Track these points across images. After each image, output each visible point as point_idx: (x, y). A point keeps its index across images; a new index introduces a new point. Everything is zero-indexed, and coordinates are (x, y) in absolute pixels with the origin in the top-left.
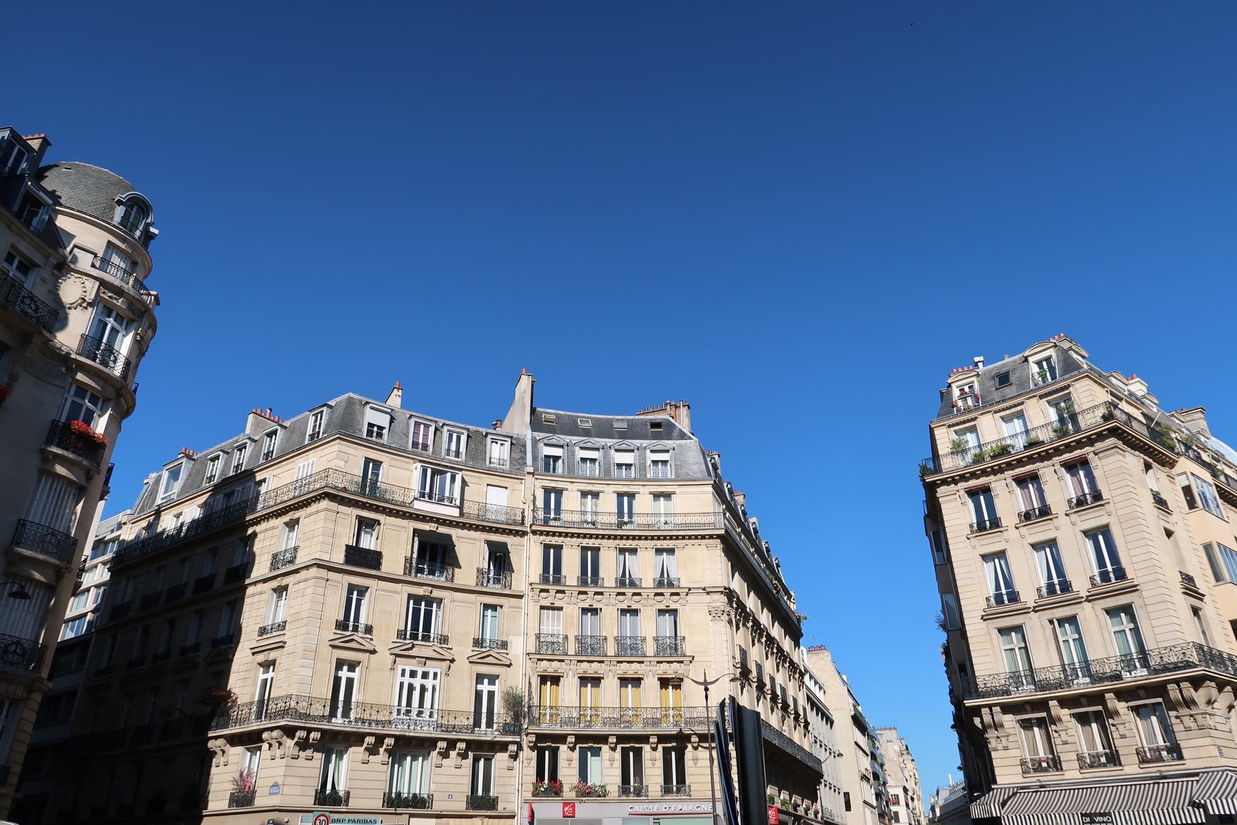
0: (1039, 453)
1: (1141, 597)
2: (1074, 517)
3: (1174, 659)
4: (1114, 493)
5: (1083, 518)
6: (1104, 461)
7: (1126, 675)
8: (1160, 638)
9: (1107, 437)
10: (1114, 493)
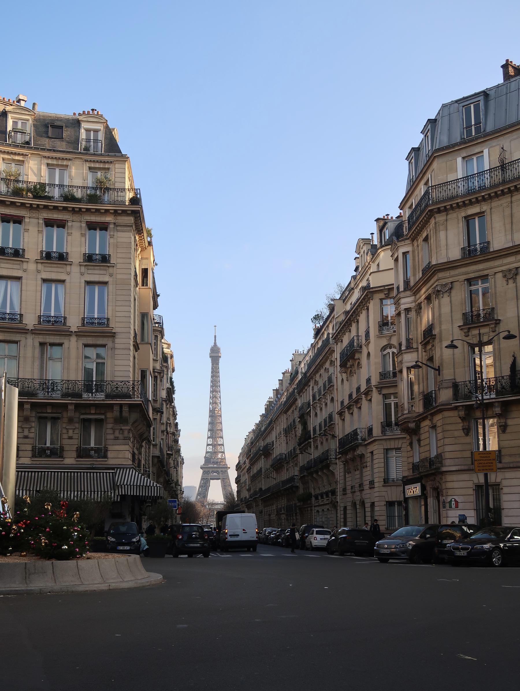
0: (73, 208)
1: (113, 342)
2: (83, 268)
3: (125, 390)
4: (119, 260)
6: (120, 234)
7: (85, 396)
8: (117, 374)
10: (119, 260)
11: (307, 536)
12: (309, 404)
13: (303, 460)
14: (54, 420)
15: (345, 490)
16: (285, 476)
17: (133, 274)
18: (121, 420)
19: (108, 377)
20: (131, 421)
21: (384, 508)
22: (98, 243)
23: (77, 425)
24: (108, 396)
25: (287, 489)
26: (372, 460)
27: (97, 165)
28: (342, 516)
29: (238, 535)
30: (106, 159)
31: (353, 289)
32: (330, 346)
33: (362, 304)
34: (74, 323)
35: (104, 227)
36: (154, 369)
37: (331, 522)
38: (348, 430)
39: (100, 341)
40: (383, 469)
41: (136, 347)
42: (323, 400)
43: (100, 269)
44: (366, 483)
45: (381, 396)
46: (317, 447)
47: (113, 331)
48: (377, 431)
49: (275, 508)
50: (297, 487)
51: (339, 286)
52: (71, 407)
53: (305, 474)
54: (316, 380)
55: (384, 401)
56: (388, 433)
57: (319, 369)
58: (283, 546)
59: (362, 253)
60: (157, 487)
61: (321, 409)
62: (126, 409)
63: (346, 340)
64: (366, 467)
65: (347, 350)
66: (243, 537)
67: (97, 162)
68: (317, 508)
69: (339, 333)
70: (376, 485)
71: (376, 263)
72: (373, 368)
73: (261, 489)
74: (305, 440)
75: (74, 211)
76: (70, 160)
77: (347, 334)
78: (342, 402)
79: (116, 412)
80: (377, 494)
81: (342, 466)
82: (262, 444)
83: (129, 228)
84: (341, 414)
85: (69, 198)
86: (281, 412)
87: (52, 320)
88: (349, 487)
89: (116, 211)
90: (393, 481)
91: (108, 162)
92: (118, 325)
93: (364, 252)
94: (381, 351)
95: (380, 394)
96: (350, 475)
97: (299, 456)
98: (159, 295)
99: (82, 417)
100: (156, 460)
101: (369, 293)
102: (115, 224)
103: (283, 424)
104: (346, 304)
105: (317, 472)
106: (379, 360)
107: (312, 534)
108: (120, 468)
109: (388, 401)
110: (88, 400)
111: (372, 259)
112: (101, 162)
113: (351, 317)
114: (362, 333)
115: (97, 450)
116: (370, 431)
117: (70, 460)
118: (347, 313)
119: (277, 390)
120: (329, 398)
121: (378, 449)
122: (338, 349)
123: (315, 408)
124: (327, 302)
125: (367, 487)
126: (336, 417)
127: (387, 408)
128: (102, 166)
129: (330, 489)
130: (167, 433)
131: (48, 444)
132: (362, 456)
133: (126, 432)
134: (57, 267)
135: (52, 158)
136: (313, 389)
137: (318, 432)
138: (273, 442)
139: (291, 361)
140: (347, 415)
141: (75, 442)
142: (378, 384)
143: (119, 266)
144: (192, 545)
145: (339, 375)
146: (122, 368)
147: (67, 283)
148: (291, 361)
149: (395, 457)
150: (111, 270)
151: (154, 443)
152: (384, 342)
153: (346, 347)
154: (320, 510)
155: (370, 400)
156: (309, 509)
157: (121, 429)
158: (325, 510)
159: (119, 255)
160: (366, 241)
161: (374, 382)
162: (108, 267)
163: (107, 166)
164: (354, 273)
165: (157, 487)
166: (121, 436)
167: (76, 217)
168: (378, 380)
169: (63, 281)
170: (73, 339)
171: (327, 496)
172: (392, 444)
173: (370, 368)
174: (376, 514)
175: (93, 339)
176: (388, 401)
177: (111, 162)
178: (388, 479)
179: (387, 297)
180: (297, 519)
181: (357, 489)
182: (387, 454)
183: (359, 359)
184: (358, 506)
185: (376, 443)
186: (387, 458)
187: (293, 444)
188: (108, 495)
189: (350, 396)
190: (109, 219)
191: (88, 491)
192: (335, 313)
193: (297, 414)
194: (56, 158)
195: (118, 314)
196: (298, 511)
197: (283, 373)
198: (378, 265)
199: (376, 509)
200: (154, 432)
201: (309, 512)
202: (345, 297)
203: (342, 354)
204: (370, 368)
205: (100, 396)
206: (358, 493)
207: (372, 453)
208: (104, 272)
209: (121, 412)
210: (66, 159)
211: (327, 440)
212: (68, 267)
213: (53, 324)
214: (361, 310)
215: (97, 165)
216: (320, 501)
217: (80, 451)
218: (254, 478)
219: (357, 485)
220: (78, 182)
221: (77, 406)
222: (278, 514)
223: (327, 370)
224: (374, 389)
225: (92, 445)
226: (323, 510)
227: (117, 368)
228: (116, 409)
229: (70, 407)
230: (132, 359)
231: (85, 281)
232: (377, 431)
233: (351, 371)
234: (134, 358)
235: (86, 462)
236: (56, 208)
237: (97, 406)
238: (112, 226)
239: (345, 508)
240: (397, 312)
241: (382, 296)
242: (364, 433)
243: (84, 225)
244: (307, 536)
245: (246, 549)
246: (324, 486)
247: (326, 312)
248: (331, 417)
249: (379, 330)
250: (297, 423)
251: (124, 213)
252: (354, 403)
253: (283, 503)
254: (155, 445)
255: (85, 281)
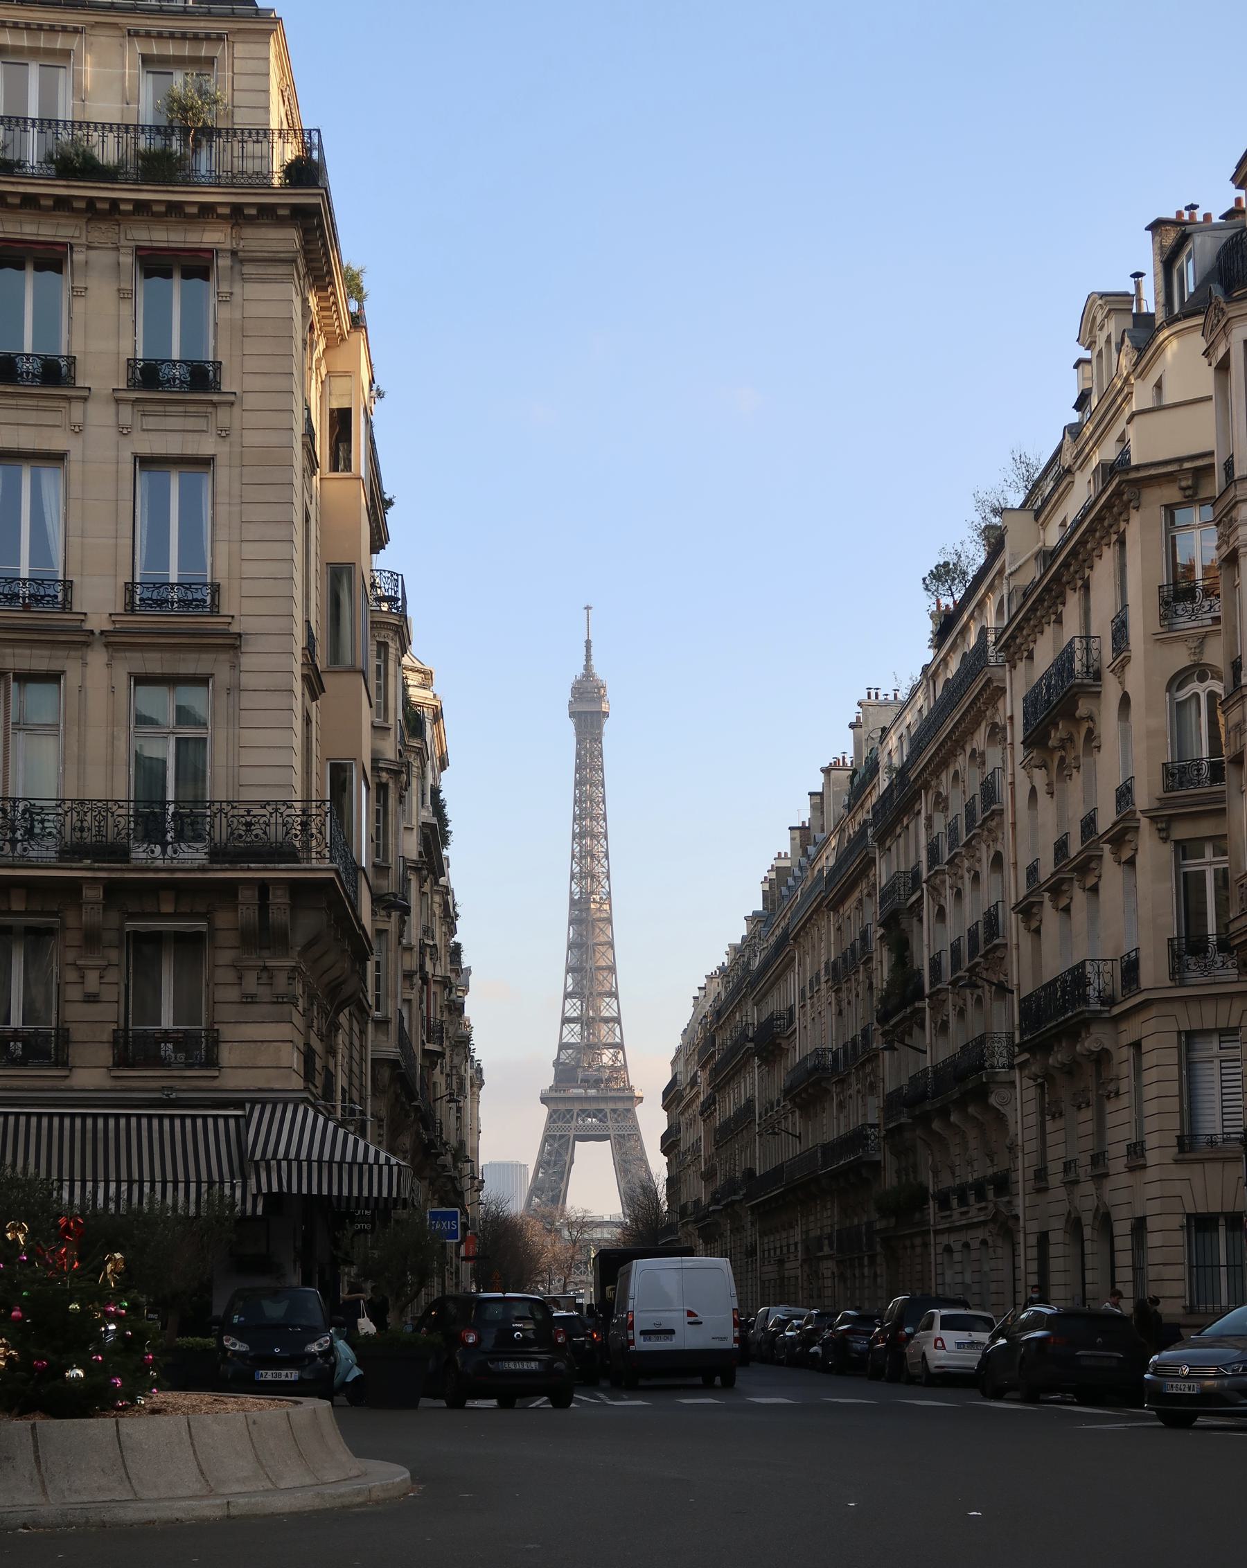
0: (91, 201)
1: (235, 666)
2: (126, 412)
4: (252, 383)
5: (151, 422)
6: (253, 290)
7: (139, 853)
8: (248, 776)
9: (280, 222)
10: (252, 383)
11: (910, 1336)
12: (916, 875)
13: (894, 1071)
14: (37, 937)
15: (1041, 1174)
16: (831, 1125)
17: (299, 429)
18: (264, 937)
19: (217, 788)
20: (299, 939)
21: (1180, 1238)
22: (178, 322)
23: (114, 955)
24: (217, 855)
25: (840, 1174)
26: (1138, 1071)
27: (171, 49)
28: (1033, 1266)
29: (672, 1332)
30: (201, 26)
31: (1069, 471)
32: (989, 673)
33: (1103, 524)
34: (98, 602)
35: (197, 266)
36: (375, 761)
37: (993, 1287)
38: (1054, 967)
39: (190, 665)
40: (1174, 1104)
41: (314, 686)
42: (966, 864)
43: (186, 415)
44: (1117, 1153)
45: (1169, 847)
46: (943, 1028)
47: (235, 629)
48: (1153, 972)
49: (798, 1238)
50: (876, 1167)
51: (1021, 460)
52: (92, 894)
53: (903, 1120)
54: (939, 794)
55: (1178, 866)
56: (1194, 977)
57: (952, 754)
58: (827, 1370)
59: (1101, 343)
60: (391, 1167)
61: (959, 895)
62: (279, 899)
63: (1045, 653)
64: (1117, 1094)
65: (1048, 687)
66: (688, 1339)
67: (172, 36)
68: (944, 1239)
69: (1019, 628)
70: (1152, 1157)
71: (1152, 378)
72: (1139, 750)
73: (750, 1173)
74: (903, 1002)
75: (93, 212)
76: (76, 31)
77: (1049, 630)
78: (1032, 871)
79: (247, 912)
80: (1154, 1190)
81: (1032, 1093)
82: (752, 1016)
83: (282, 270)
84: (1027, 910)
85: (74, 165)
86: (820, 905)
87: (24, 591)
88: (1055, 1168)
89: (237, 209)
90: (1212, 1143)
91: (208, 38)
92: (249, 607)
93: (1108, 341)
94: (1168, 689)
95: (1165, 840)
96: (1060, 1123)
97: (881, 1057)
98: (389, 503)
99: (131, 925)
100: (386, 1073)
101: (1124, 484)
102: (234, 253)
103: (825, 946)
104: (1044, 526)
105: (944, 1113)
106: (1163, 720)
107: (929, 1326)
108: (264, 1102)
109: (1192, 865)
110: (148, 870)
111: (1136, 364)
112: (184, 37)
113: (1064, 573)
114: (1102, 626)
115: (184, 1042)
116: (1131, 968)
117: (91, 1074)
118: (1046, 556)
119: (803, 829)
120: (985, 855)
121: (1157, 1034)
122: (1018, 685)
123: (935, 891)
124: (977, 519)
125: (1118, 1164)
126: (1012, 923)
127: (1190, 887)
128: (186, 50)
129: (990, 1171)
130: (425, 981)
131: (16, 1021)
132: (1102, 1058)
133: (281, 979)
134: (37, 409)
135: (15, 26)
136: (929, 826)
137: (947, 975)
138: (791, 1010)
139: (852, 726)
140: (1049, 917)
141: (108, 1012)
142: (1156, 804)
143: (250, 401)
144: (512, 1365)
145: (1021, 774)
146: (265, 756)
147: (74, 466)
148: (852, 726)
149: (1217, 1061)
150: (223, 416)
151: (377, 1014)
152: (1180, 658)
153: (1047, 676)
154: (957, 1247)
155: (1131, 862)
156: (918, 1241)
157: (265, 968)
158: (975, 1244)
159: (251, 364)
160: (1116, 303)
161: (1143, 799)
162: (215, 404)
163: (204, 50)
164: (1075, 417)
165: (391, 1167)
166: (264, 992)
167: (101, 233)
168: (1159, 791)
169: (58, 458)
170: (97, 658)
171: (981, 1197)
172: (1208, 1017)
173: (1129, 751)
174: (1153, 1257)
175: (167, 656)
176: (1192, 865)
177: (220, 38)
178: (1193, 1136)
179: (1191, 498)
180: (876, 1275)
181: (1084, 1171)
182: (1189, 1050)
183: (1090, 718)
184: (1087, 1232)
185: (1153, 1011)
186: (1191, 1065)
187: (860, 1016)
188: (222, 1196)
189: (1061, 847)
190: (214, 237)
191: (153, 1182)
192: (1006, 555)
193: (872, 912)
194: (28, 27)
195: (250, 569)
196: (879, 1249)
197: (826, 771)
198: (1158, 386)
199: (1153, 1240)
200: (378, 978)
201: (918, 1250)
202: (1039, 503)
203: (1031, 702)
204: (1129, 751)
205: (193, 855)
206: (1088, 1188)
207: (1137, 1045)
208: (199, 423)
209: (264, 907)
210: (64, 30)
211: (979, 1001)
212: (77, 410)
213: (26, 608)
214: (1099, 545)
215: (171, 49)
216: (956, 1215)
217: (126, 1043)
218: (725, 1135)
219: (1085, 1159)
220: (106, 109)
221: (113, 889)
222: (811, 1259)
223: (978, 758)
224: (1144, 823)
225: (167, 1022)
226: (966, 1245)
227: (248, 758)
228: (248, 896)
229: (90, 894)
230: (298, 725)
231: (136, 457)
232: (1153, 972)
233: (1062, 759)
234: (308, 721)
235: (145, 1080)
236: (30, 202)
237: (184, 889)
238: (224, 262)
239: (1043, 1238)
240: (1225, 550)
241: (1172, 494)
242: (1107, 977)
243: (127, 260)
244: (910, 1336)
245: (699, 1380)
246: (970, 1163)
247: (975, 556)
248: (992, 921)
249: (1163, 617)
250: (875, 945)
251: (267, 214)
252: (1074, 871)
253: (826, 1219)
254: (382, 1024)
255: (136, 457)
